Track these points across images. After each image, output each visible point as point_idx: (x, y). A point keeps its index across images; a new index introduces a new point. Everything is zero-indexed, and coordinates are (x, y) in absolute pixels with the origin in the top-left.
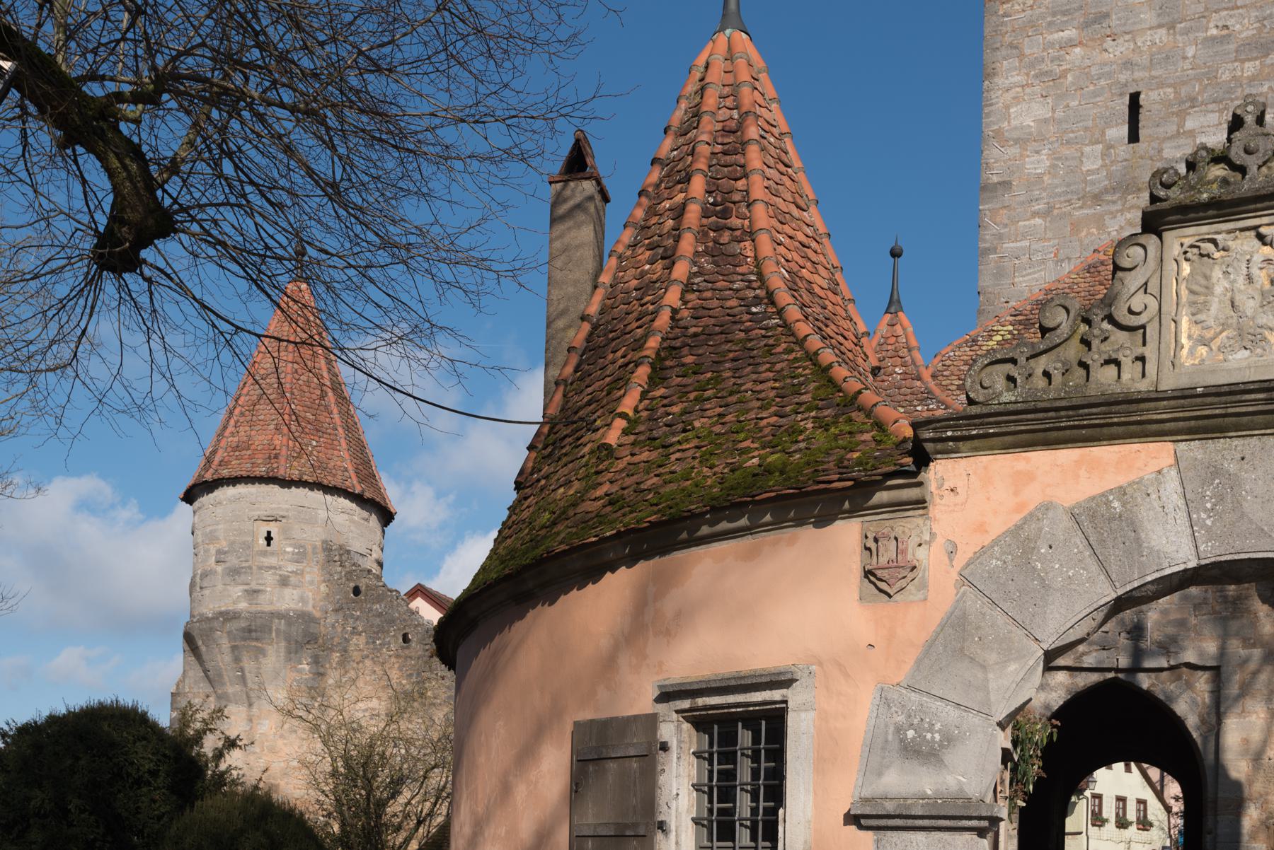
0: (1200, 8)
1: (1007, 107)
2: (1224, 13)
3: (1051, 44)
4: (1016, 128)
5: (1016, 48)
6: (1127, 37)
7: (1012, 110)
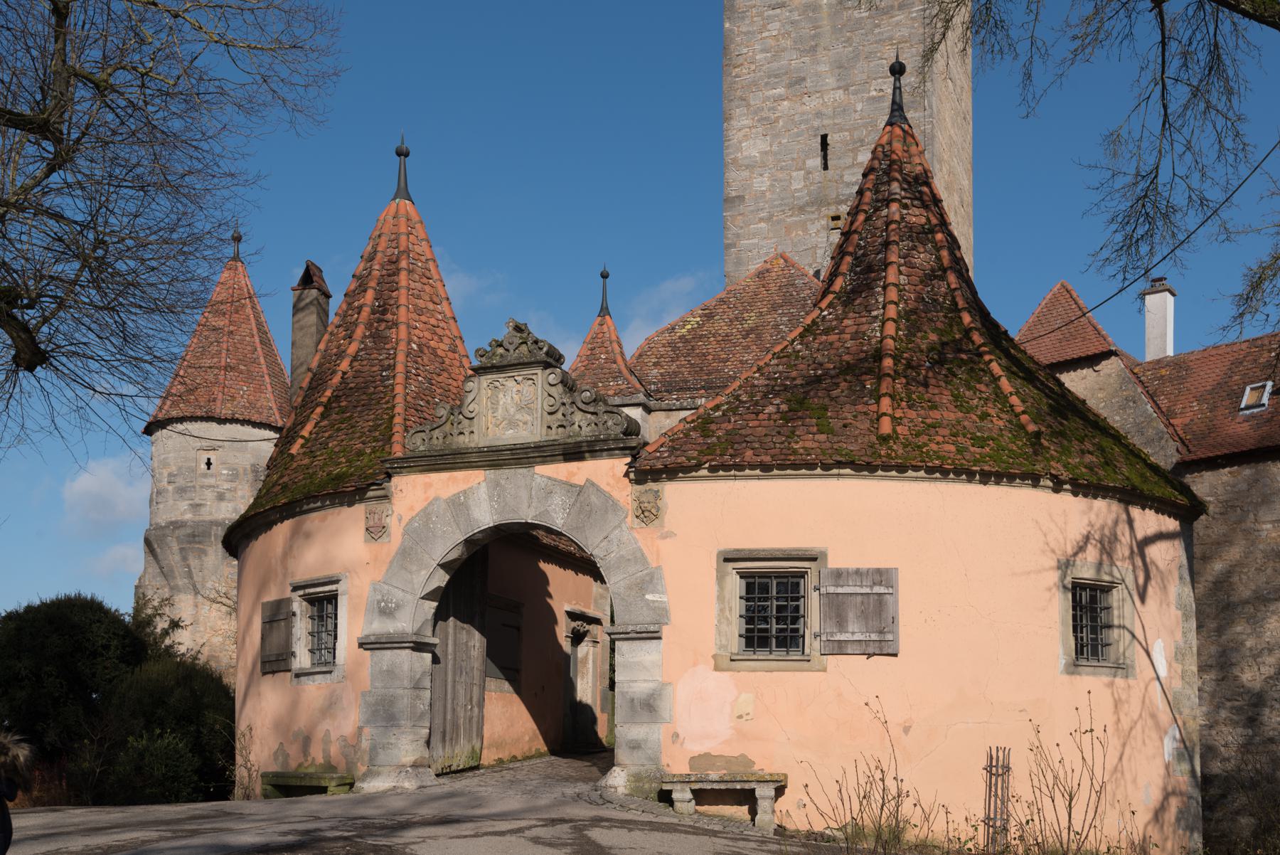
1: (740, 142)
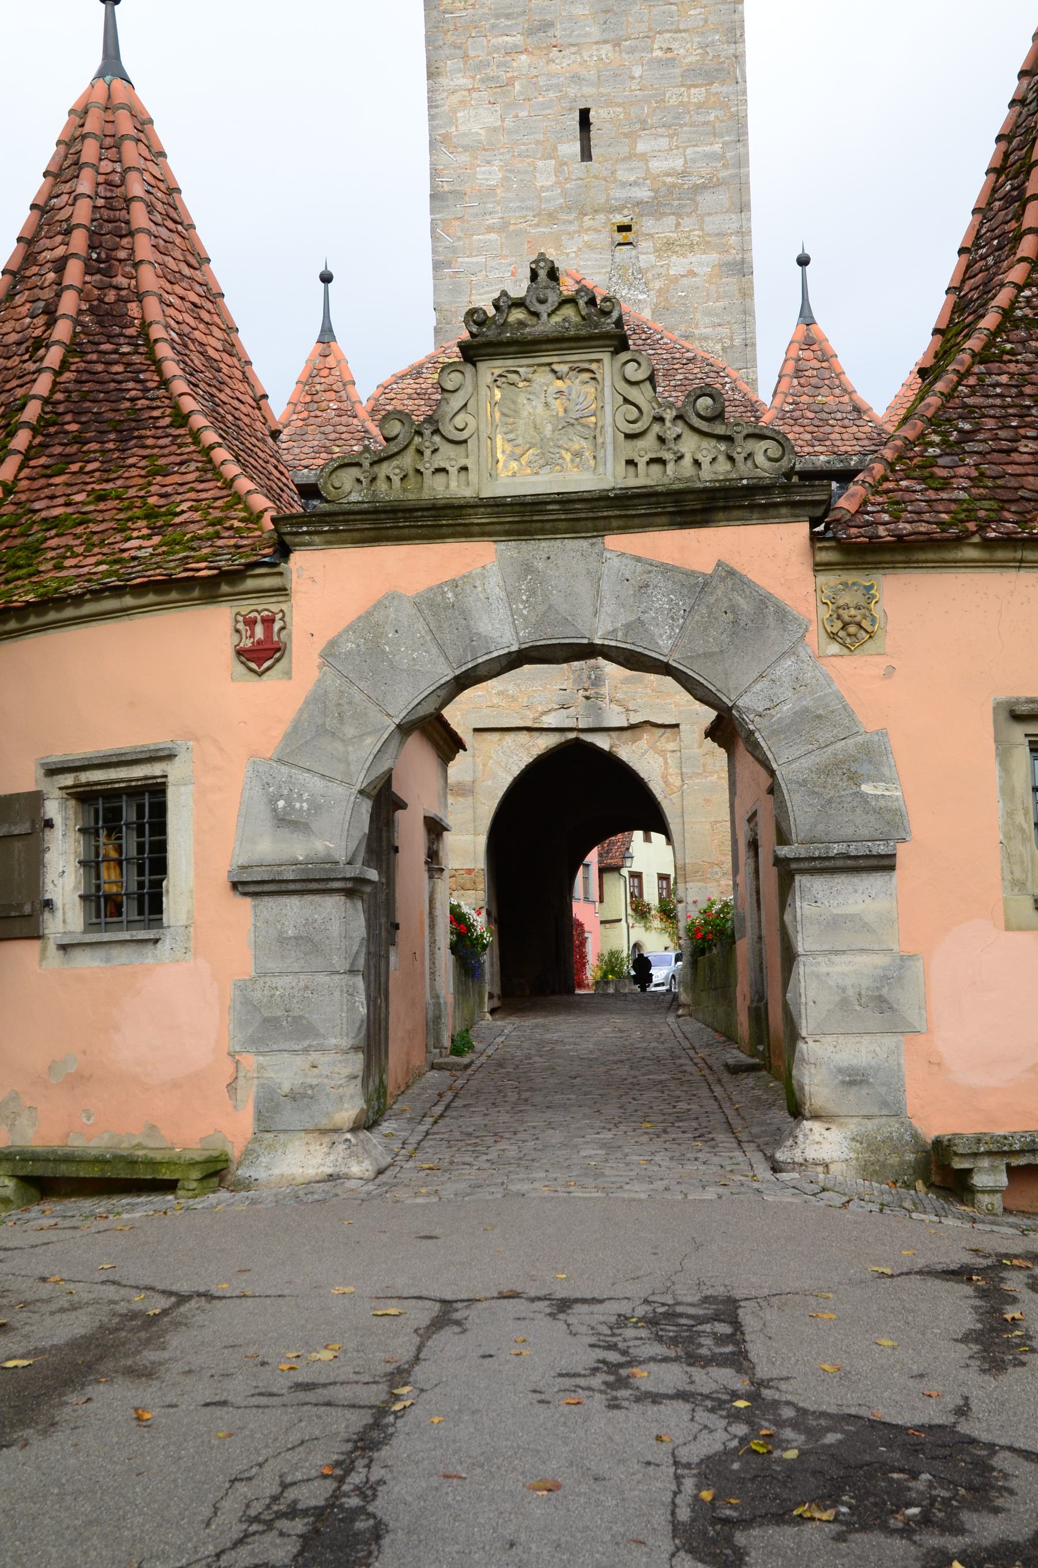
0: (644, 27)
1: (454, 111)
2: (667, 35)
3: (497, 49)
4: (464, 134)
5: (459, 48)
6: (574, 49)
7: (459, 115)
